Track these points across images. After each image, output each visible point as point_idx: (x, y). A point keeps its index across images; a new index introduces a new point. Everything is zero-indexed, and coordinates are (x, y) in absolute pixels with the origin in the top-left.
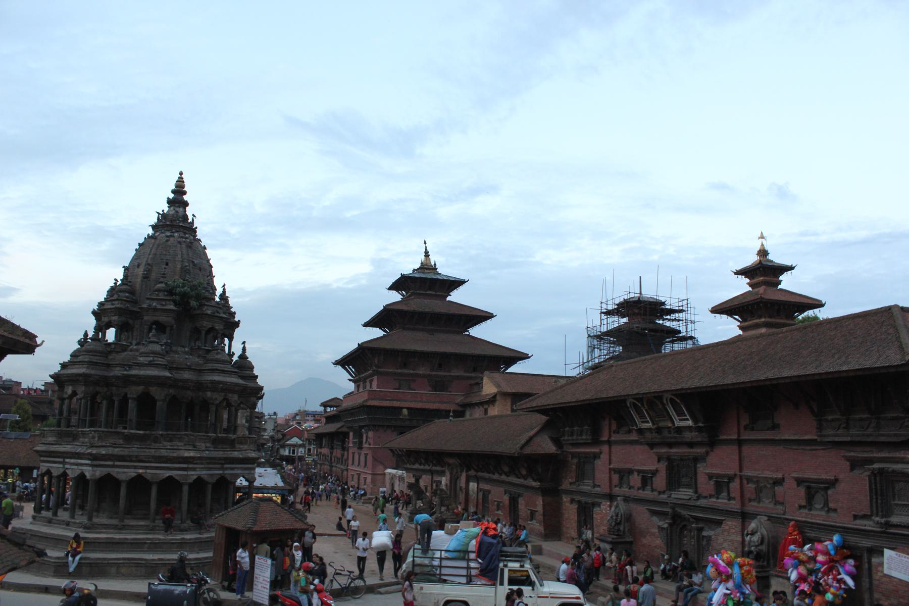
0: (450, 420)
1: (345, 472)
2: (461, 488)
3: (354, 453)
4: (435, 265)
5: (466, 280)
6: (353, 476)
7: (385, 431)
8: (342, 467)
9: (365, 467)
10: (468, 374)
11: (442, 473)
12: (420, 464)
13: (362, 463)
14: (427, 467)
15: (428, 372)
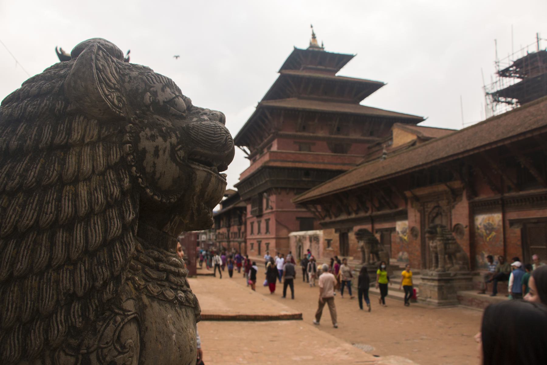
0: (385, 158)
1: (243, 244)
2: (457, 229)
3: (252, 224)
4: (322, 45)
5: (354, 54)
6: (252, 245)
7: (287, 194)
8: (239, 240)
9: (266, 233)
10: (366, 138)
11: (403, 215)
12: (349, 214)
13: (263, 230)
14: (362, 214)
15: (327, 135)
